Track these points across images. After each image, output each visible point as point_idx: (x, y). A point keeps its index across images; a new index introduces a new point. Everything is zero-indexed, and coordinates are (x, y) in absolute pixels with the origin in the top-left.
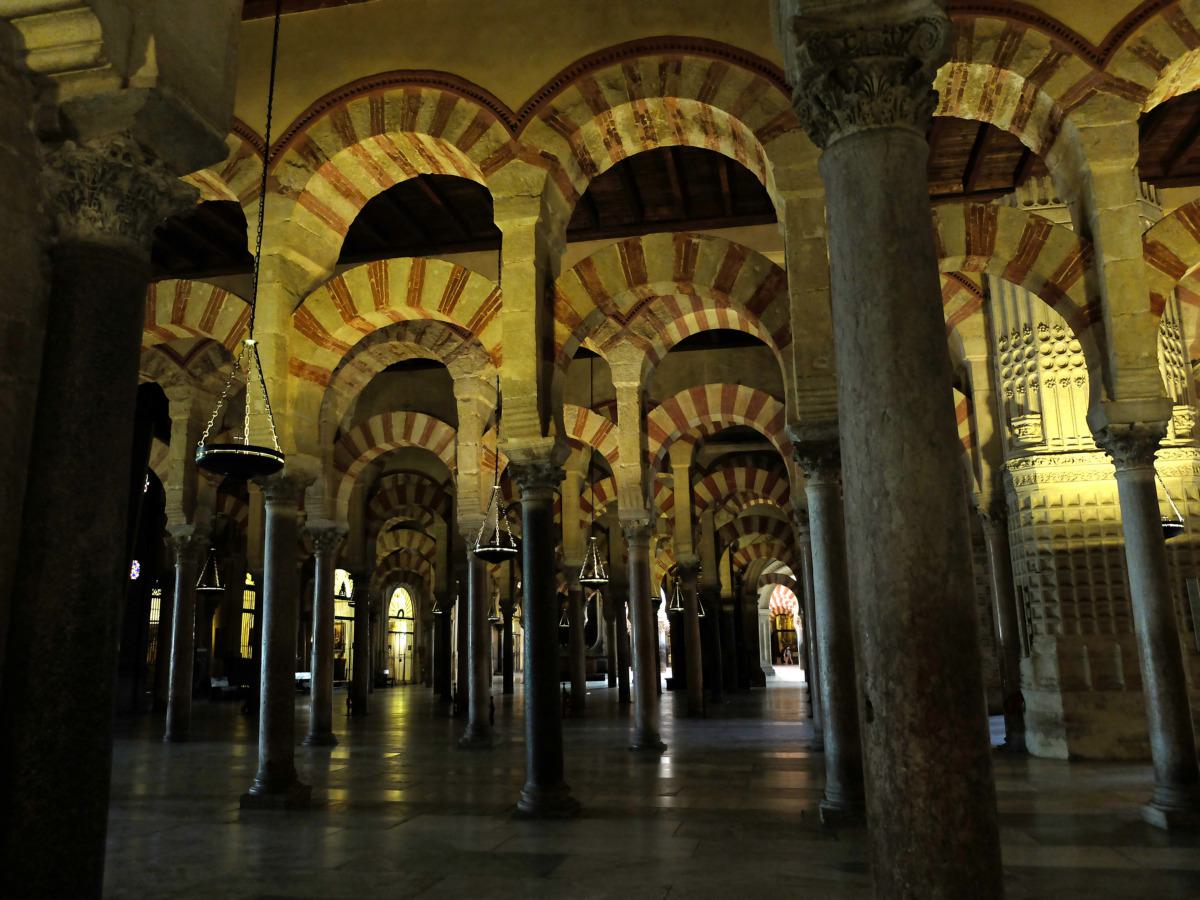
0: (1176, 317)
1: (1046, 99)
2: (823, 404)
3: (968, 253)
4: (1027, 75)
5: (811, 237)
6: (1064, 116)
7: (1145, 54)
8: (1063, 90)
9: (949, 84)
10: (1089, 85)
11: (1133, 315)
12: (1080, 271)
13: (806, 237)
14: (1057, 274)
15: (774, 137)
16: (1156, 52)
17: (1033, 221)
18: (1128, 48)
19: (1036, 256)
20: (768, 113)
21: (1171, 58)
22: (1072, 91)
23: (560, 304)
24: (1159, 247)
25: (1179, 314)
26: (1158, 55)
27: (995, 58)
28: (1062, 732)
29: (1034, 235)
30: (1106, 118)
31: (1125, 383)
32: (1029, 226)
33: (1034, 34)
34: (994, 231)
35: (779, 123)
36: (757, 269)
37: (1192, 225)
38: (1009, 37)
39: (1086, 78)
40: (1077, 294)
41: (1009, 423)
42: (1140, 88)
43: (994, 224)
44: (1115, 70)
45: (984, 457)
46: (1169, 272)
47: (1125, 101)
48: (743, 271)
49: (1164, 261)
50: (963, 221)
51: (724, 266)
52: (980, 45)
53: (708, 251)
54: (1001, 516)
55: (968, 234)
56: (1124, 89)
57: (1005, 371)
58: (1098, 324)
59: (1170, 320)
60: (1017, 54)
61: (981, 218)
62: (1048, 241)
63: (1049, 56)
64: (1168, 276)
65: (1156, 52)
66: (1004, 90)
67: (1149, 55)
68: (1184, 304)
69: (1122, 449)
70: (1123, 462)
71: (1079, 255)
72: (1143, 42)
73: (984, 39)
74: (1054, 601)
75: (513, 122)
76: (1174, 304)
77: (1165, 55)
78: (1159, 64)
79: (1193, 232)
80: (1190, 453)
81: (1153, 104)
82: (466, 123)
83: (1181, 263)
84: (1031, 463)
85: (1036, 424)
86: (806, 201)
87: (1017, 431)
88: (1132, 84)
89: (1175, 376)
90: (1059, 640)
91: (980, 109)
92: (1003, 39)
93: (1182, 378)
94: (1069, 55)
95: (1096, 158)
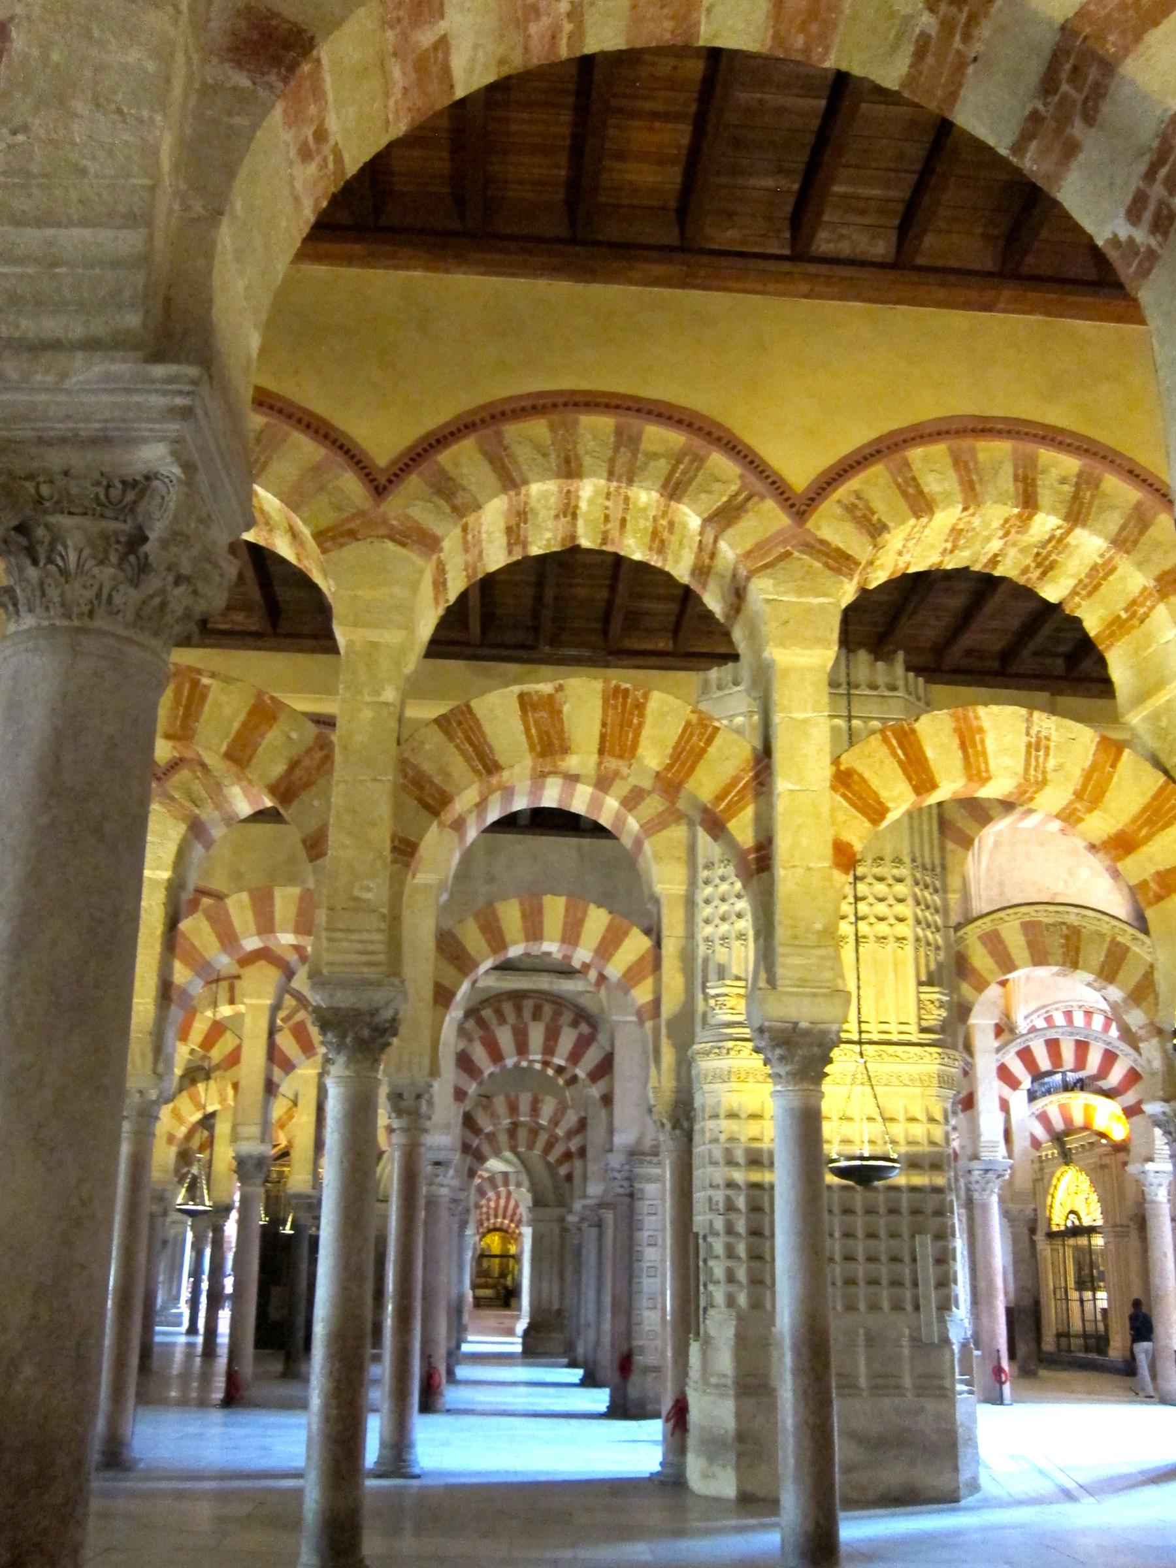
0: (937, 861)
1: (728, 552)
2: (361, 953)
3: (601, 752)
4: (706, 516)
5: (376, 699)
6: (748, 578)
7: (859, 514)
8: (749, 545)
9: (607, 508)
10: (785, 542)
11: (809, 869)
12: (750, 796)
13: (368, 698)
14: (719, 798)
15: (342, 545)
16: (873, 513)
17: (694, 718)
18: (839, 502)
19: (692, 769)
20: (339, 509)
21: (891, 524)
22: (761, 547)
24: (856, 777)
25: (943, 858)
26: (876, 517)
27: (665, 486)
28: (732, 1456)
29: (695, 738)
30: (800, 592)
31: (789, 964)
32: (688, 724)
33: (719, 461)
34: (641, 725)
35: (352, 525)
36: (294, 735)
37: (900, 752)
38: (687, 459)
39: (780, 532)
40: (742, 829)
41: (704, 987)
42: (848, 557)
43: (642, 715)
44: (819, 528)
45: (669, 1037)
46: (864, 813)
47: (829, 573)
48: (273, 737)
49: (860, 798)
50: (599, 703)
51: (244, 725)
52: (646, 464)
53: (223, 699)
54: (686, 1125)
55: (604, 725)
56: (828, 555)
57: (707, 911)
58: (764, 875)
59: (929, 866)
60: (694, 484)
61: (624, 704)
62: (712, 750)
63: (737, 494)
64: (864, 819)
65: (873, 513)
66: (677, 530)
67: (864, 516)
68: (950, 846)
69: (782, 1058)
70: (780, 1076)
71: (751, 774)
72: (859, 497)
73: (654, 456)
74: (739, 1258)
76: (936, 842)
77: (884, 519)
78: (875, 530)
79: (900, 762)
80: (936, 1056)
81: (877, 579)
83: (881, 803)
84: (724, 1051)
85: (739, 995)
86: (375, 645)
87: (712, 1002)
88: (838, 550)
89: (928, 944)
90: (740, 1318)
91: (651, 549)
92: (679, 461)
93: (938, 948)
94: (763, 498)
95: (782, 644)
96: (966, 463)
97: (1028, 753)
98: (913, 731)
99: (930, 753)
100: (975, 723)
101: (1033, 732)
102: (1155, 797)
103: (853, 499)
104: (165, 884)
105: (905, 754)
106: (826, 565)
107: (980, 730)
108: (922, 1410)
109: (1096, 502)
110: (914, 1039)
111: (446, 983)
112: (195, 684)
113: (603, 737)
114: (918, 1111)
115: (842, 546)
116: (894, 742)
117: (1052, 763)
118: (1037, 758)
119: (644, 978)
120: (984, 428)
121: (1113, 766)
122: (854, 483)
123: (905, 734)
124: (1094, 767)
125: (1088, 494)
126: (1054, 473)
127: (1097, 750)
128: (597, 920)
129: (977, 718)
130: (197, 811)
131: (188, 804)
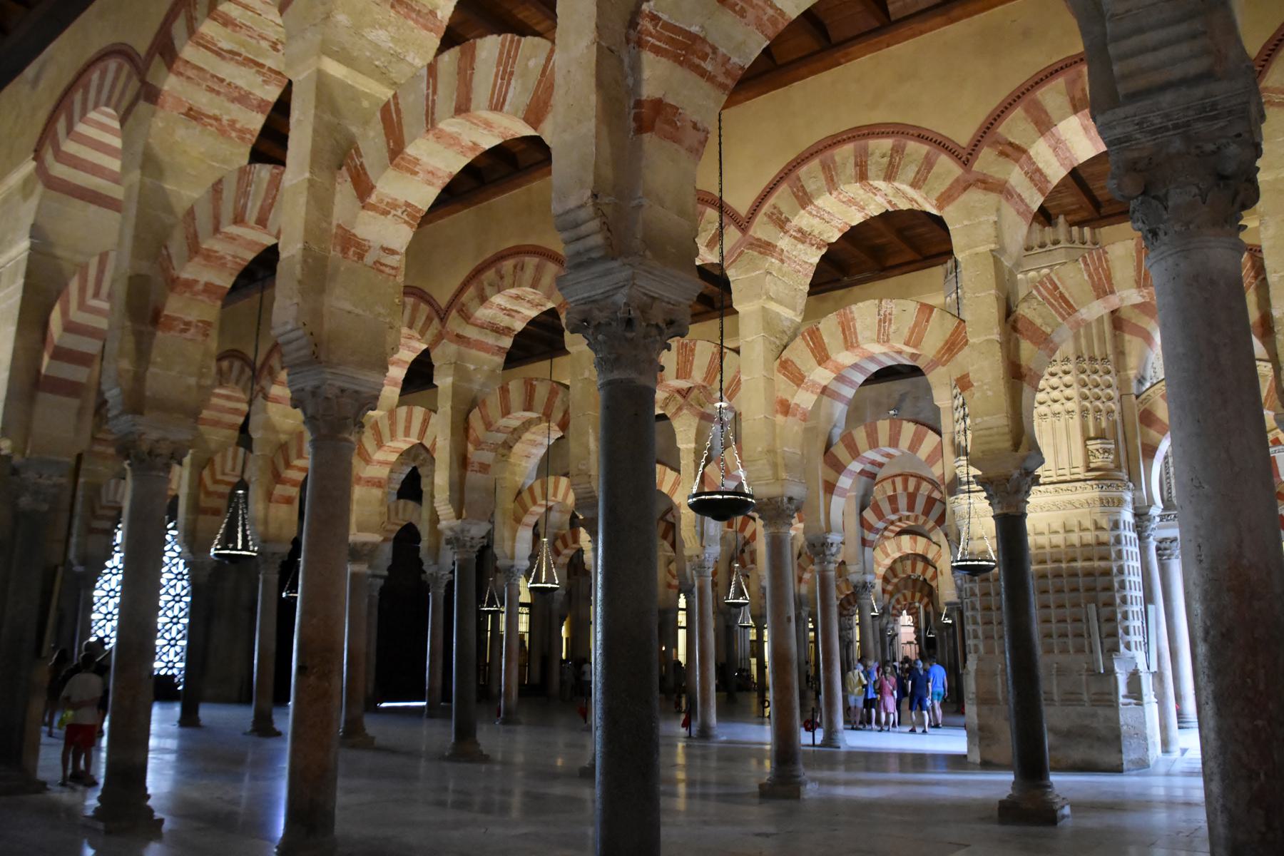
13: (580, 378)
16: (781, 214)
18: (765, 214)
21: (790, 218)
23: (471, 431)
26: (784, 215)
32: (713, 353)
34: (693, 359)
37: (811, 343)
42: (768, 244)
43: (693, 355)
44: (755, 232)
47: (761, 256)
49: (792, 374)
51: (548, 399)
55: (678, 364)
56: (760, 247)
65: (781, 214)
72: (775, 208)
75: (442, 316)
80: (1095, 486)
82: (424, 318)
83: (801, 374)
96: (829, 167)
97: (880, 326)
98: (818, 329)
99: (826, 340)
100: (850, 316)
101: (882, 313)
102: (952, 335)
103: (772, 210)
104: (693, 450)
105: (814, 343)
106: (760, 253)
107: (853, 319)
108: (1094, 715)
109: (902, 163)
110: (1081, 477)
111: (830, 479)
112: (531, 385)
113: (678, 370)
114: (1088, 523)
115: (766, 239)
116: (808, 338)
117: (893, 327)
118: (884, 327)
119: (938, 460)
120: (836, 141)
121: (927, 321)
122: (772, 200)
123: (814, 332)
124: (916, 325)
125: (898, 159)
126: (878, 153)
127: (918, 313)
128: (908, 429)
129: (851, 312)
130: (702, 410)
131: (699, 407)
